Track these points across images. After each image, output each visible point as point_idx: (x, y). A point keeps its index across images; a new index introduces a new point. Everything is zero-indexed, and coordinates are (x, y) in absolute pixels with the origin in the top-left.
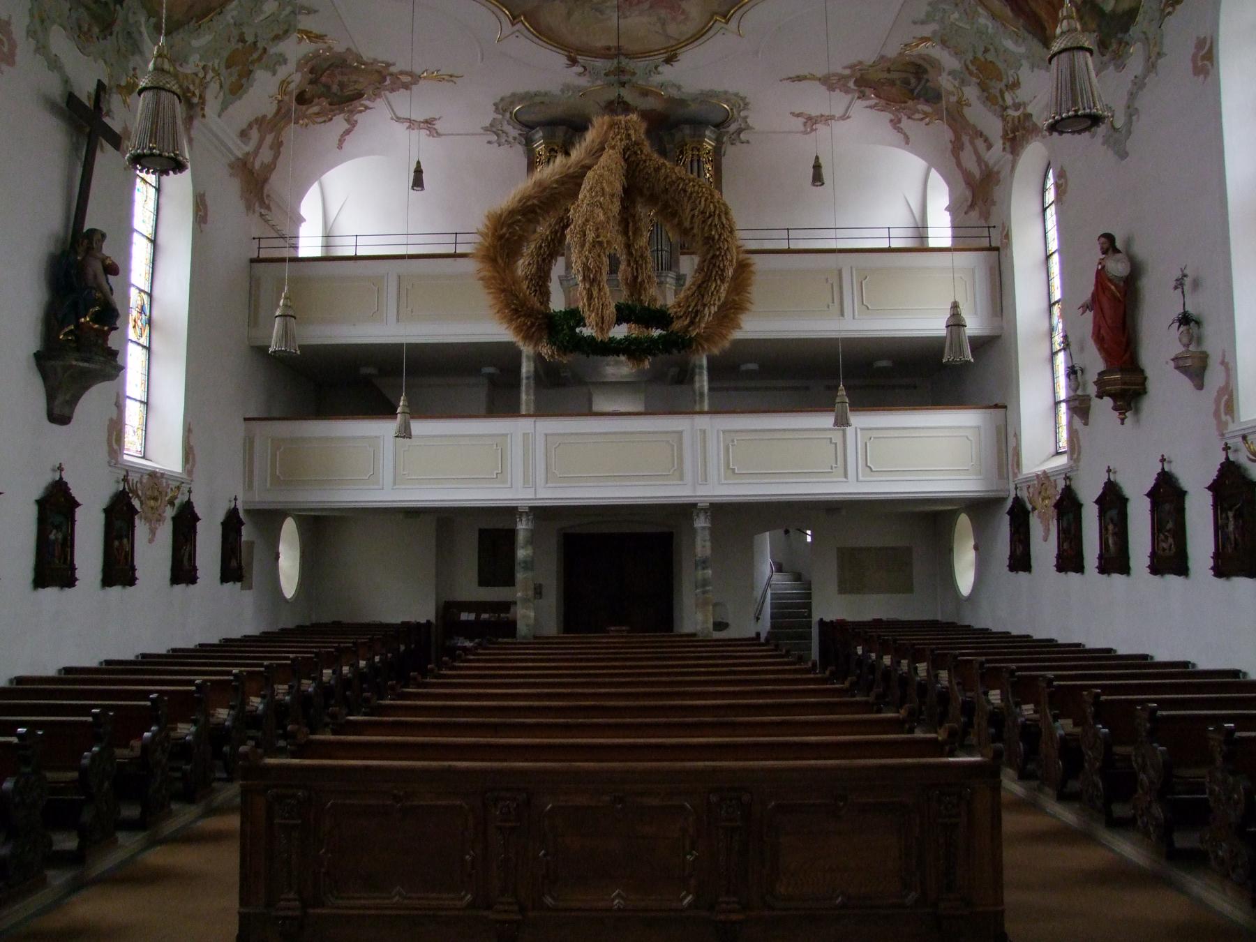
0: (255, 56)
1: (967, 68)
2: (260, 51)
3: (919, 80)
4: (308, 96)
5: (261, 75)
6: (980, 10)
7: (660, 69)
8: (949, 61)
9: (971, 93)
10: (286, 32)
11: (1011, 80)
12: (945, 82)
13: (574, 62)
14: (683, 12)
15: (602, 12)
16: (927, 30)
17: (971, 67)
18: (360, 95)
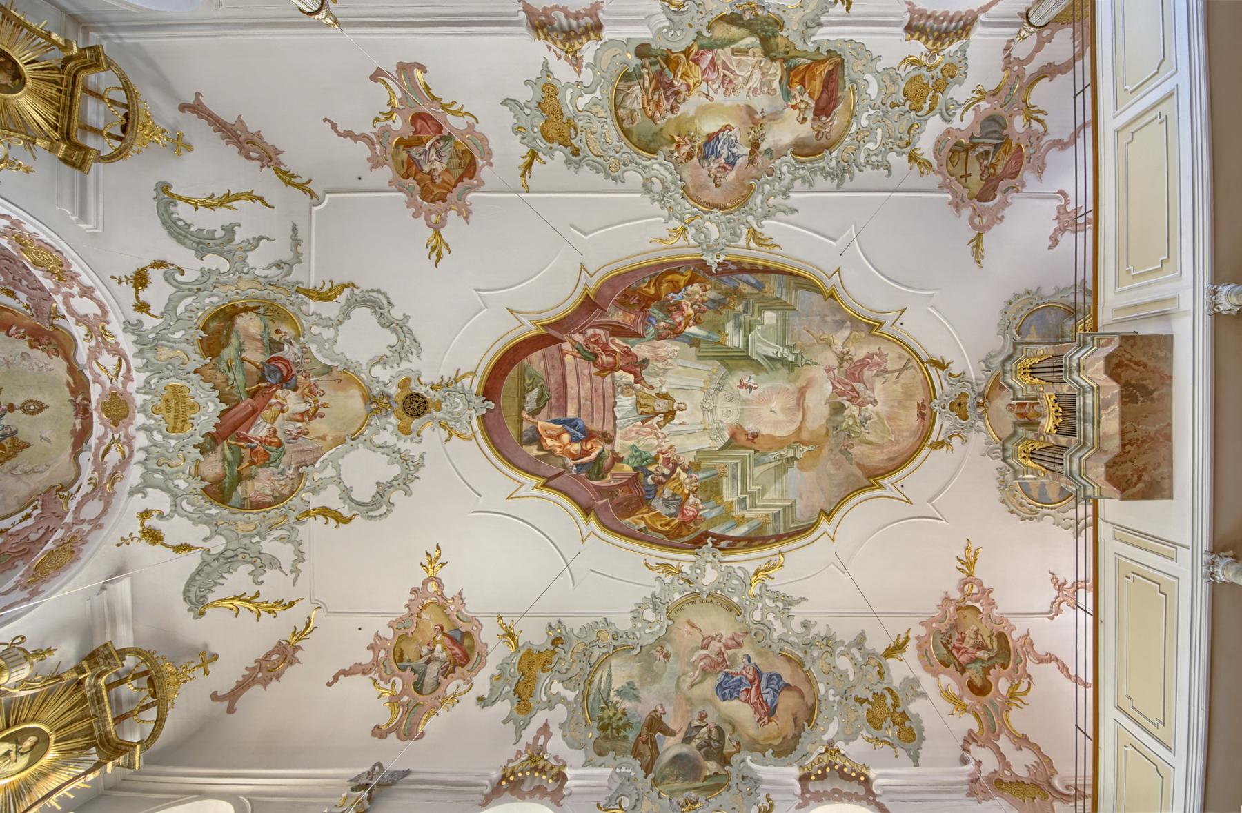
0: (889, 700)
1: (931, 109)
2: (886, 692)
3: (975, 146)
4: (978, 682)
5: (914, 708)
6: (853, 129)
7: (955, 373)
8: (934, 127)
9: (960, 92)
10: (880, 666)
11: (909, 68)
12: (964, 122)
13: (940, 444)
14: (870, 356)
15: (866, 420)
16: (898, 161)
17: (927, 107)
18: (1002, 637)
